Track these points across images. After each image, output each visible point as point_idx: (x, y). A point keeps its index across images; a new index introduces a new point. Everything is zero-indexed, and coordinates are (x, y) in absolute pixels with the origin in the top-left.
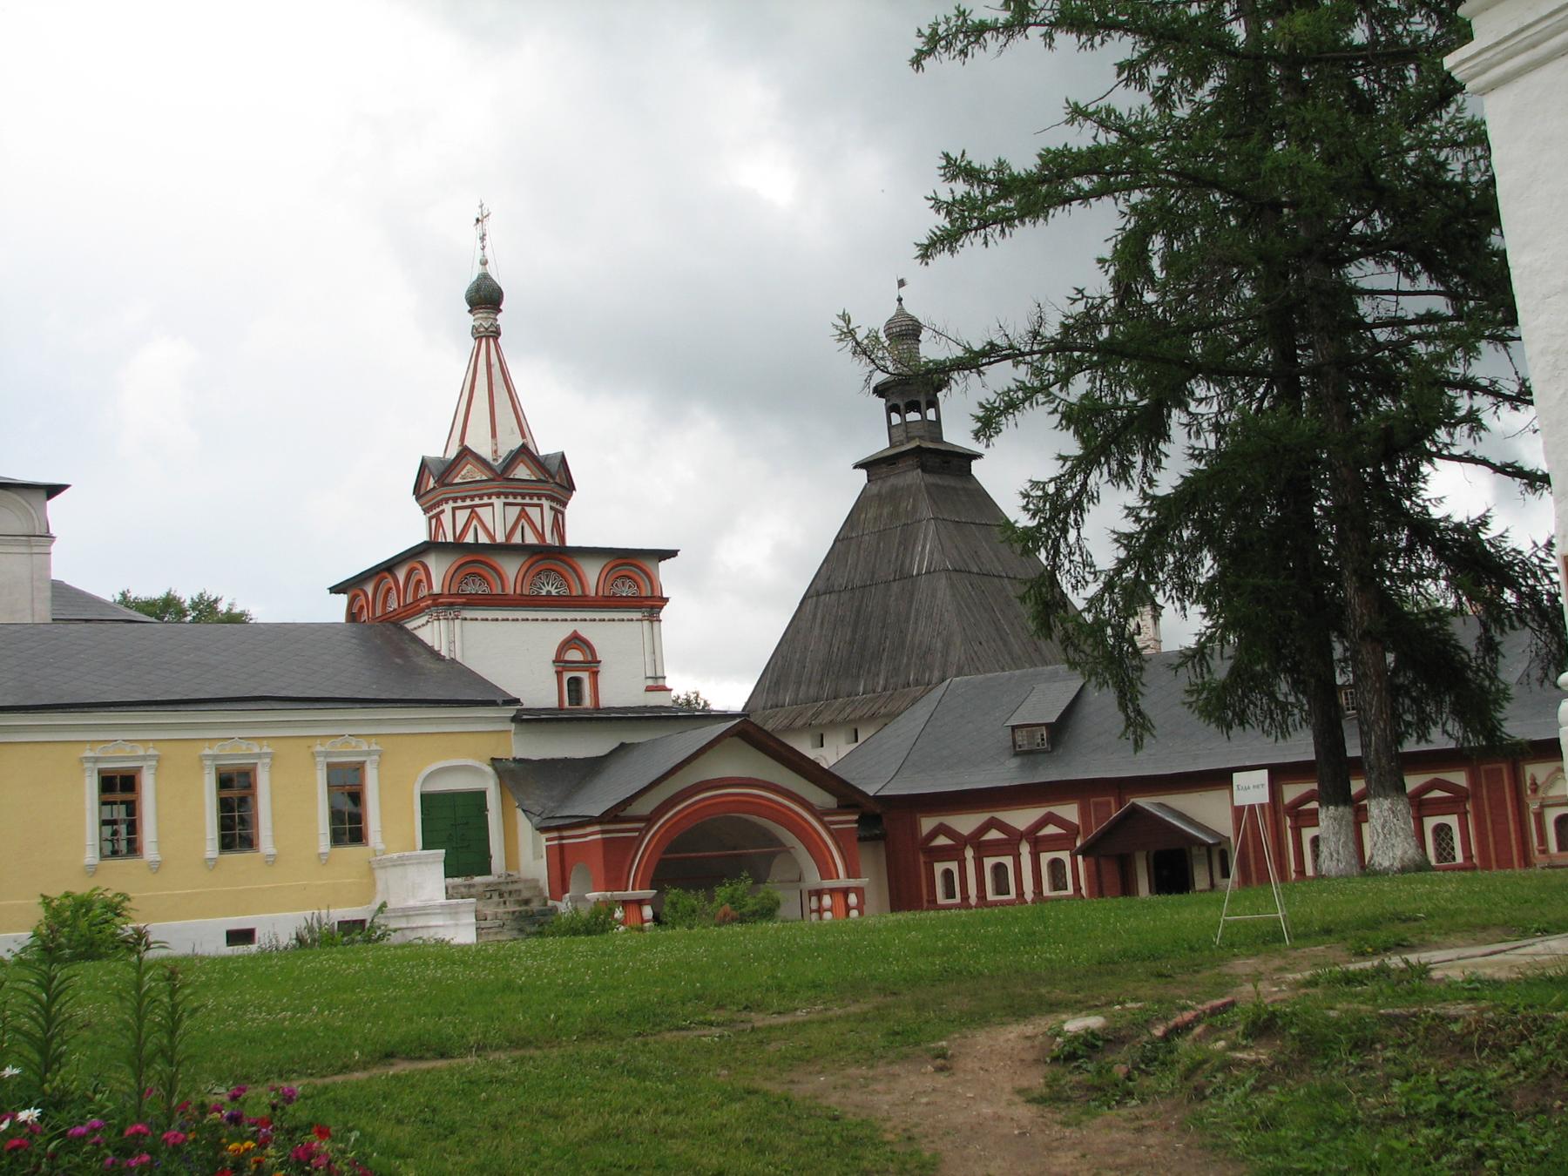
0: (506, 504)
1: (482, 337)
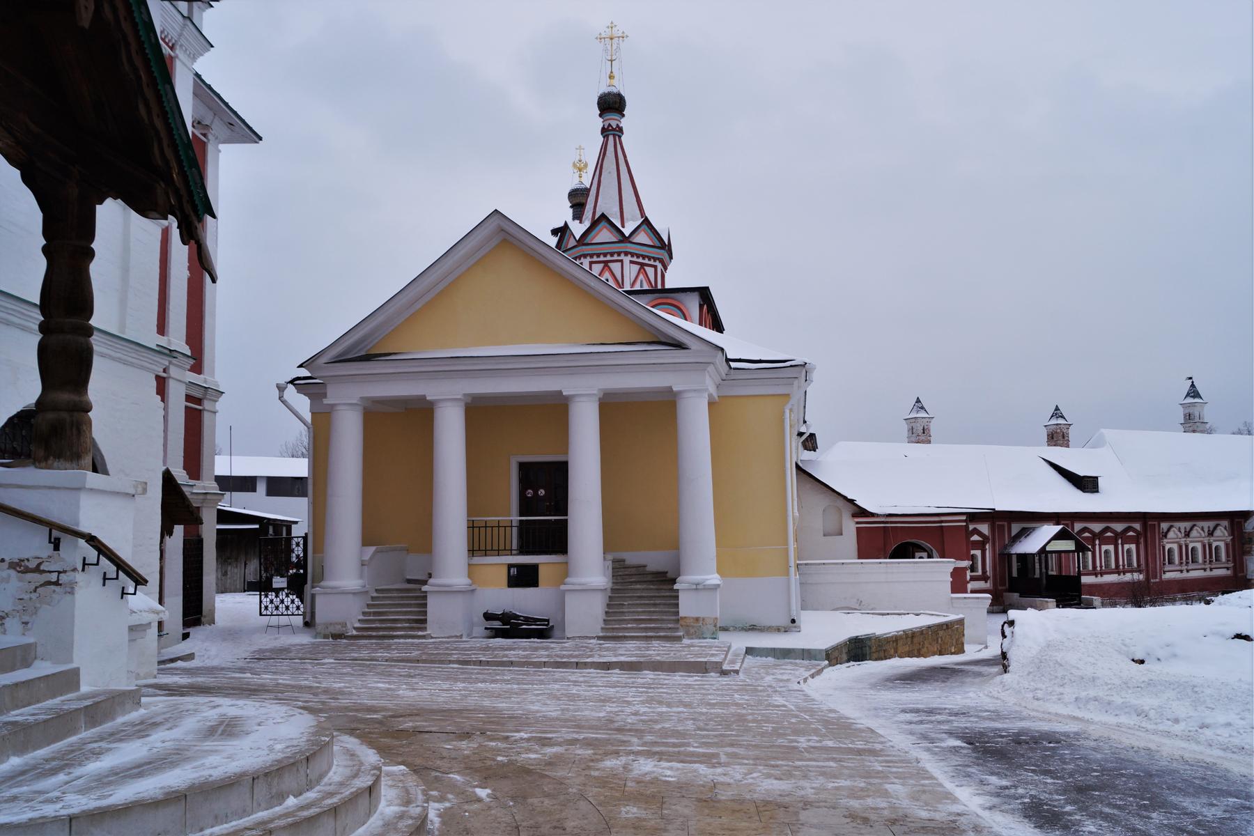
0: (632, 262)
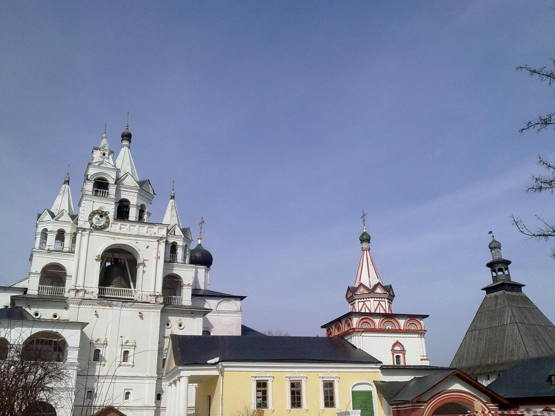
0: (374, 301)
1: (365, 250)
